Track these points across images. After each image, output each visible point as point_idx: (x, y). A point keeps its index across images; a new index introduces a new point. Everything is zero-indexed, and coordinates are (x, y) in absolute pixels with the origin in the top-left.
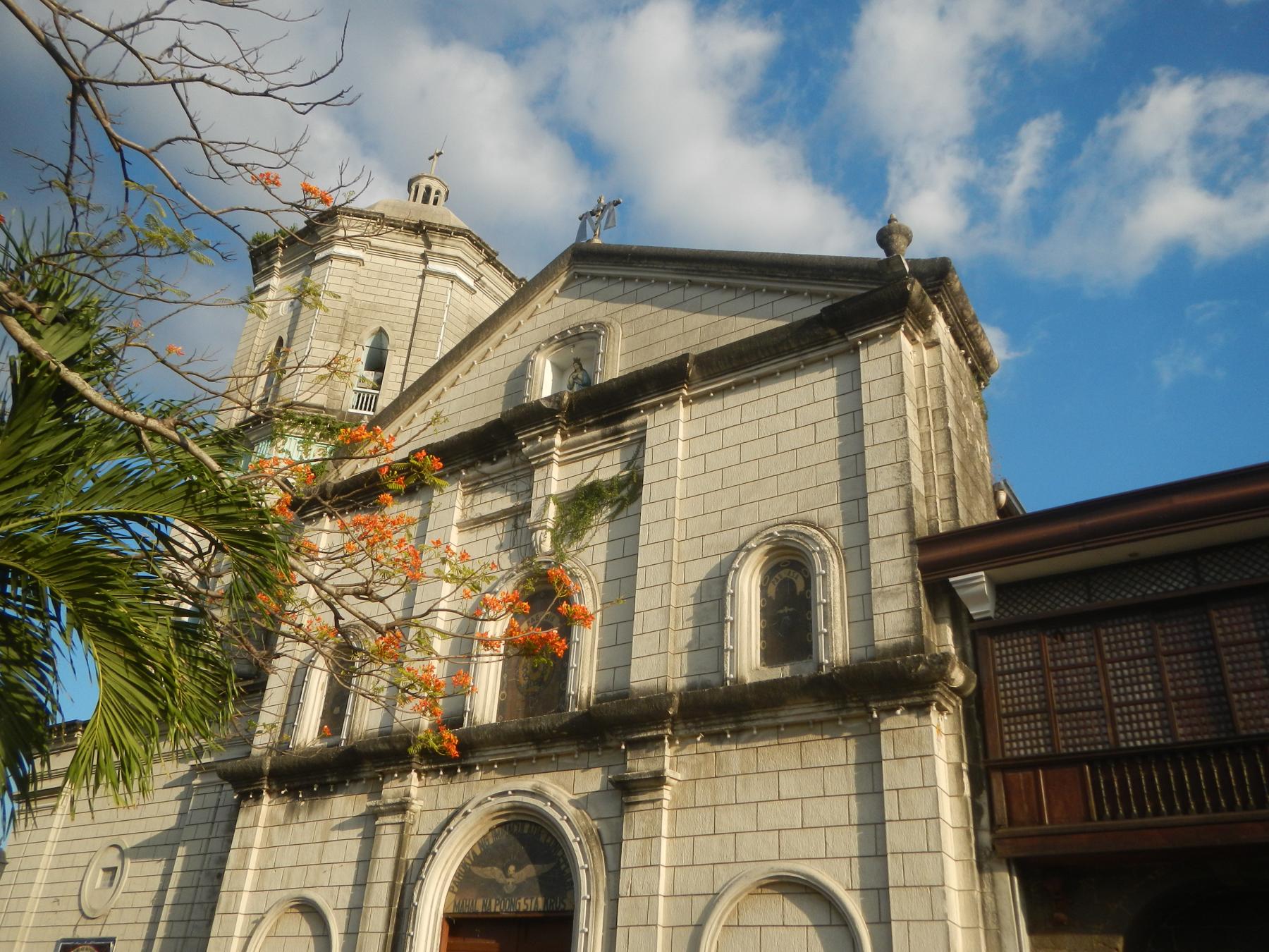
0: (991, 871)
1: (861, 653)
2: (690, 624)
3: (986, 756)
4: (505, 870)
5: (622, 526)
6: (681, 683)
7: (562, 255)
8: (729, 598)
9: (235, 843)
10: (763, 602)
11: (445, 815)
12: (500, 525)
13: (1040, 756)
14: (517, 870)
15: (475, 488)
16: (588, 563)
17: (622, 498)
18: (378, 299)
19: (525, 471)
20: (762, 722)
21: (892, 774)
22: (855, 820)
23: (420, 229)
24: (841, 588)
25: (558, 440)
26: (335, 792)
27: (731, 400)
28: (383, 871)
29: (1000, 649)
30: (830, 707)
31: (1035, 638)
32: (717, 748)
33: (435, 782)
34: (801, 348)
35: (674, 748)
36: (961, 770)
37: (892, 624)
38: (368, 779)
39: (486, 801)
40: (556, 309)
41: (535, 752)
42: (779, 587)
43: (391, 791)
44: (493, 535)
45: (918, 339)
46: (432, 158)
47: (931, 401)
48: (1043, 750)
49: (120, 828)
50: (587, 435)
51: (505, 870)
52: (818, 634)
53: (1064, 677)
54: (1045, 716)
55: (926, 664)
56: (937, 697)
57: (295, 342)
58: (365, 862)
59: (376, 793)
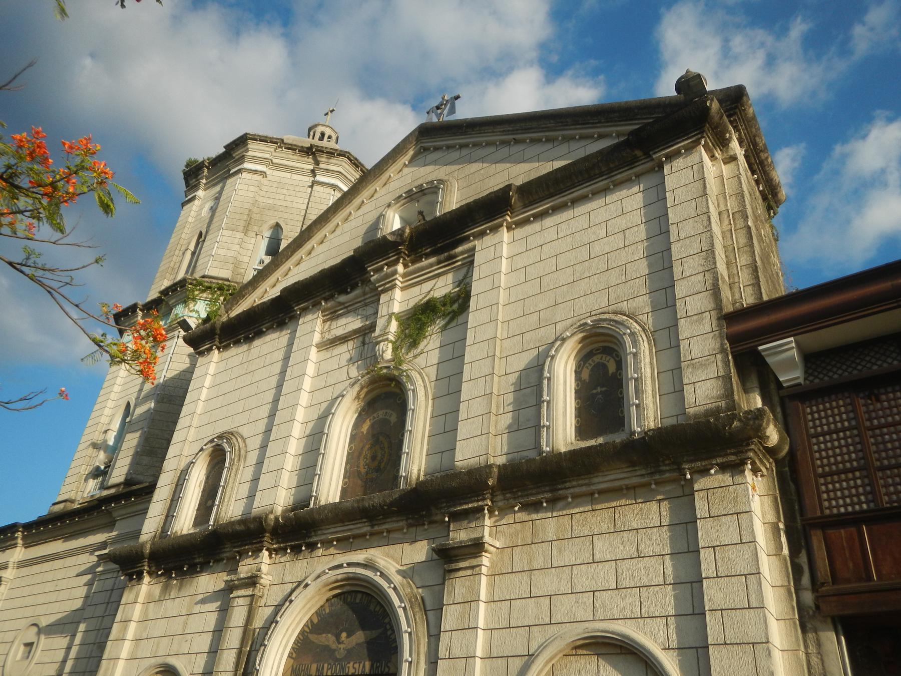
0: (816, 631)
1: (672, 421)
2: (511, 408)
3: (802, 515)
4: (338, 637)
5: (452, 334)
6: (501, 460)
7: (411, 134)
8: (545, 382)
9: (118, 618)
10: (578, 385)
11: (289, 588)
12: (351, 343)
13: (862, 512)
14: (348, 637)
15: (333, 316)
16: (422, 370)
17: (453, 311)
18: (276, 202)
19: (373, 297)
20: (577, 490)
21: (706, 533)
22: (670, 579)
23: (310, 152)
24: (651, 364)
25: (400, 268)
26: (201, 572)
27: (548, 221)
28: (233, 638)
29: (812, 413)
30: (643, 472)
31: (848, 401)
32: (534, 516)
33: (283, 559)
34: (611, 170)
35: (494, 519)
36: (779, 530)
37: (703, 390)
38: (229, 559)
39: (324, 573)
40: (405, 176)
41: (366, 529)
42: (592, 370)
43: (245, 569)
44: (345, 351)
45: (717, 155)
46: (326, 114)
47: (732, 205)
48: (865, 506)
49: (40, 610)
50: (425, 262)
51: (338, 637)
52: (629, 406)
53: (882, 435)
54: (865, 473)
55: (740, 420)
56: (751, 454)
57: (210, 232)
58: (219, 632)
59: (234, 571)
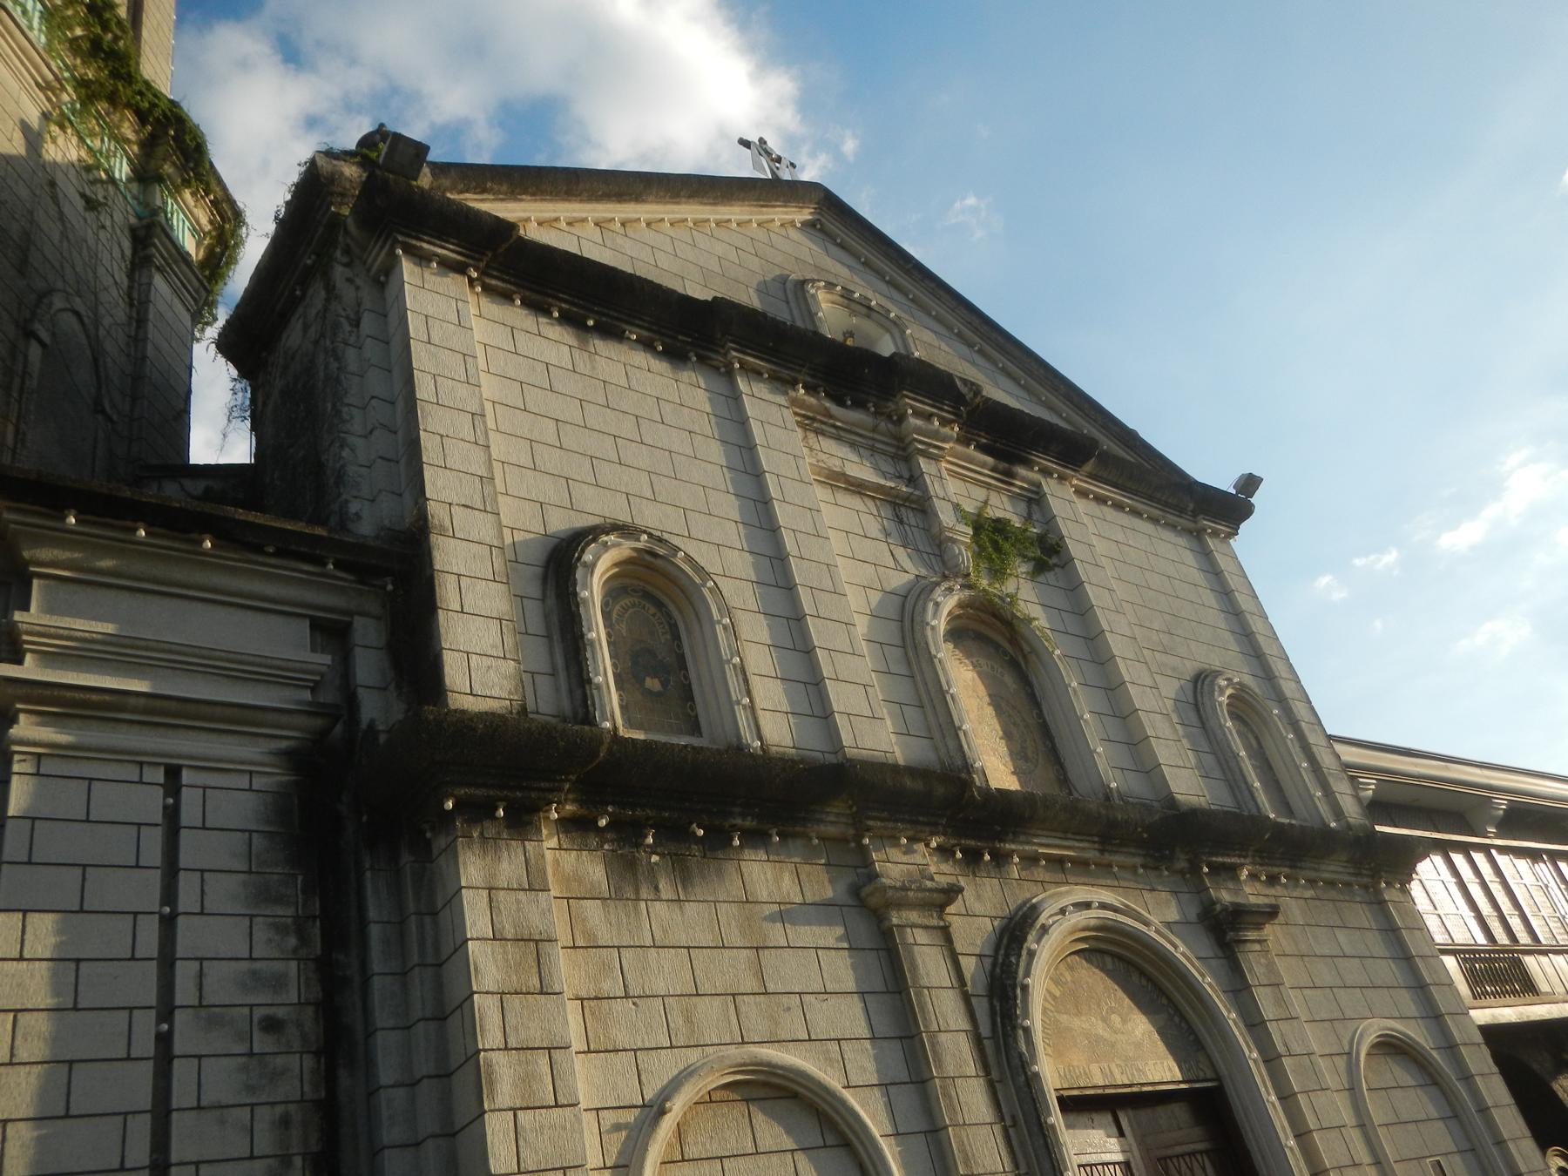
12: (870, 503)
34: (1166, 504)
